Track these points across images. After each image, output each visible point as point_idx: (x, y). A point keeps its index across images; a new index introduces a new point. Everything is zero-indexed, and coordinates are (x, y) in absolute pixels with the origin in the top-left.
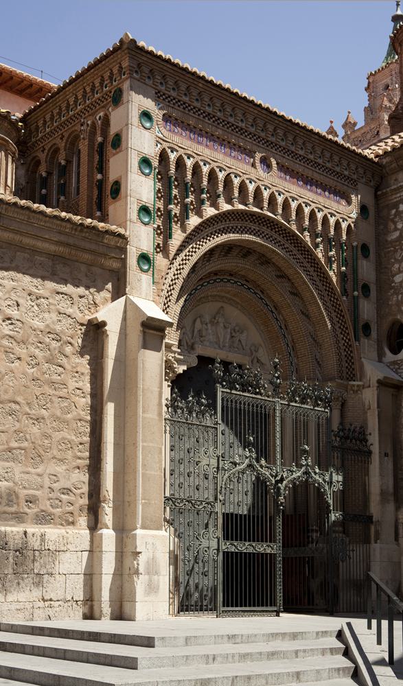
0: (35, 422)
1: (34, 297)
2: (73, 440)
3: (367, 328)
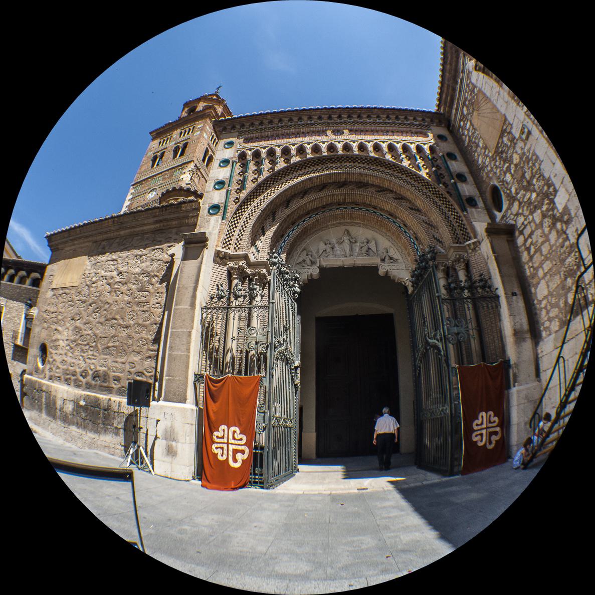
0: (125, 329)
1: (139, 257)
2: (148, 338)
3: (471, 202)
